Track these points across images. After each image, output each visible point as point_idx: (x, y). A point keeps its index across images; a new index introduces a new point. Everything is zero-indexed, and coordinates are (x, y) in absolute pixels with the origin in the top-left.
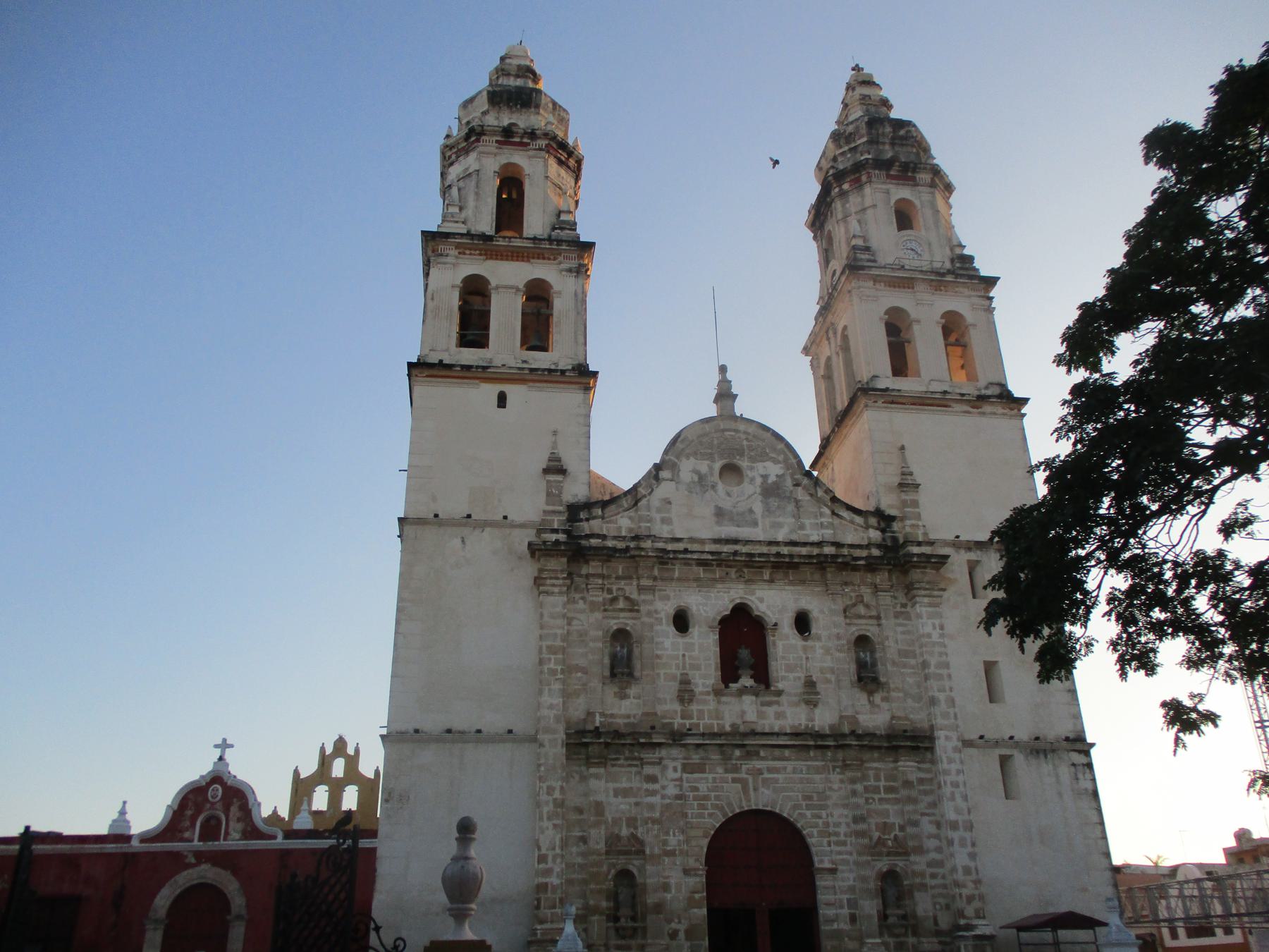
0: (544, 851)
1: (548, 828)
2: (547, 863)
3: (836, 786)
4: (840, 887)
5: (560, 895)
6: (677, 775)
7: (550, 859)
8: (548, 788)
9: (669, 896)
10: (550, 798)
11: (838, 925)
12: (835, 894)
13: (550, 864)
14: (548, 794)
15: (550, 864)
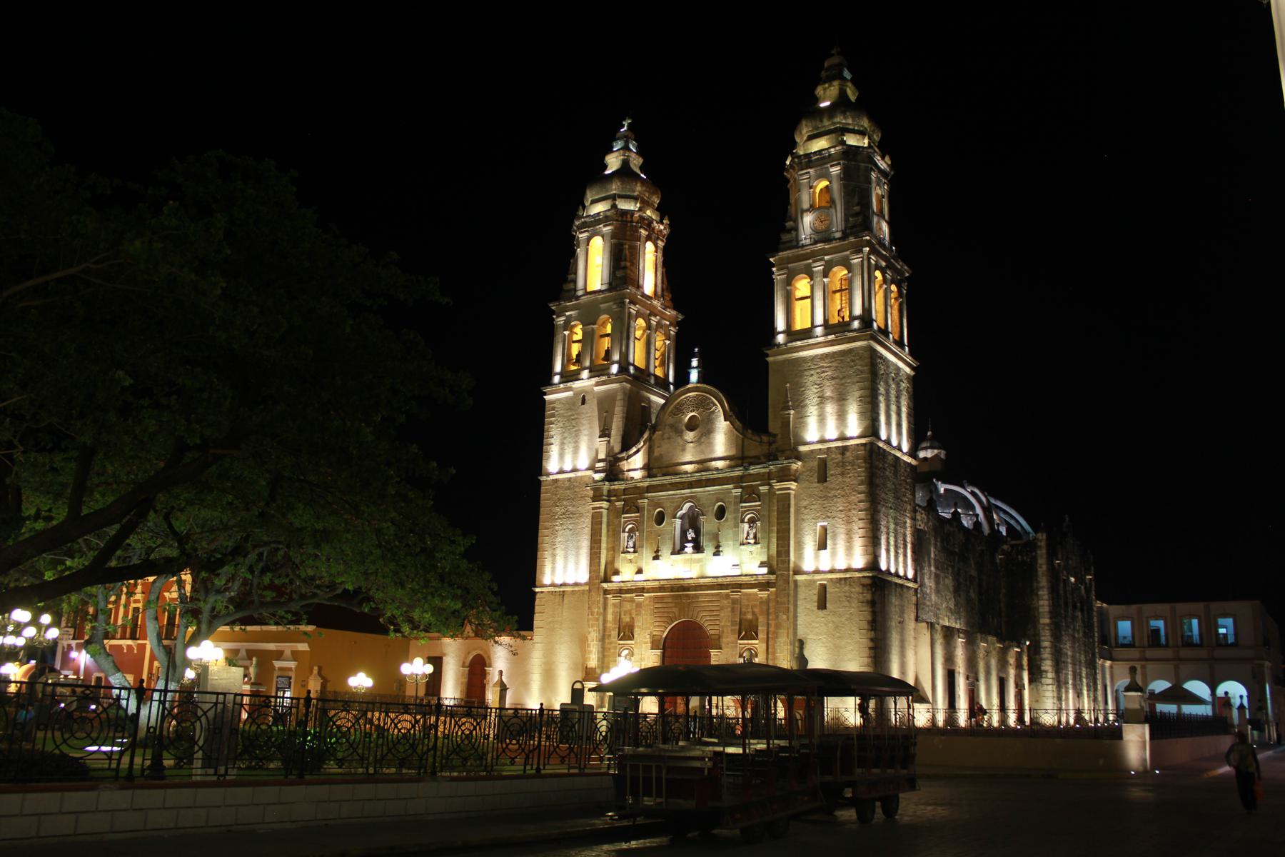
7: (592, 646)
14: (592, 615)
15: (592, 649)
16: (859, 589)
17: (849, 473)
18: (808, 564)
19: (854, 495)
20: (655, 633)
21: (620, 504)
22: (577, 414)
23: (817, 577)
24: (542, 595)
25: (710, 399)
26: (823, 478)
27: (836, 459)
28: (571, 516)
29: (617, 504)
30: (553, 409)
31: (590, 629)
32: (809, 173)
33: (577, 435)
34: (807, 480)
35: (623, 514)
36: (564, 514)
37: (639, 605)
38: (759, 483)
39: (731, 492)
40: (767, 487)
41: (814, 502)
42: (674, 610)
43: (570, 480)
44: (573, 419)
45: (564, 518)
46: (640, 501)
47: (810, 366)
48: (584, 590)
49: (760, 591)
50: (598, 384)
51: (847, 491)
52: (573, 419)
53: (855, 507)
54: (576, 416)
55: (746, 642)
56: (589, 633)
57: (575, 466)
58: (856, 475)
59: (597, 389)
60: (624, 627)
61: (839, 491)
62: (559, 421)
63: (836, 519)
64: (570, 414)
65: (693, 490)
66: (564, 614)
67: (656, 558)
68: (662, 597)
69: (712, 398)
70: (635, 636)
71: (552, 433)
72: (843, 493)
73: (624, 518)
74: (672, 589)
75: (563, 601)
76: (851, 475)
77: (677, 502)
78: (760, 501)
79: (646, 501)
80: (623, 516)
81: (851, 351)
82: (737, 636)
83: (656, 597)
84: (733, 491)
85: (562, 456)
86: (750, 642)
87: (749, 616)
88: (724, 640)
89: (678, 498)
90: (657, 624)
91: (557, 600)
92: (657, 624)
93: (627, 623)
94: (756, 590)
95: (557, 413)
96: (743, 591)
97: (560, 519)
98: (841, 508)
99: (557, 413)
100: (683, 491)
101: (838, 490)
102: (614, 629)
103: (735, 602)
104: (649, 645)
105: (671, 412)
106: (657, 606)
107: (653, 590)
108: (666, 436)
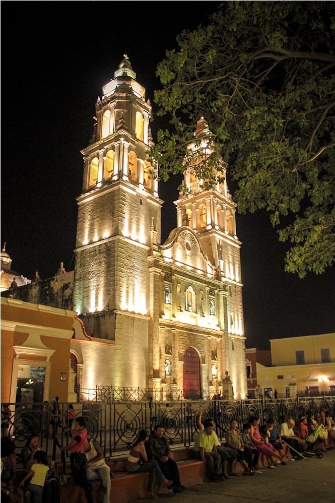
16: (241, 344)
18: (229, 332)
20: (180, 352)
23: (232, 336)
24: (120, 317)
30: (125, 196)
33: (138, 221)
36: (132, 266)
37: (174, 335)
38: (215, 288)
42: (188, 341)
43: (135, 246)
48: (146, 320)
50: (149, 197)
56: (154, 347)
57: (138, 239)
59: (148, 200)
64: (134, 205)
65: (193, 281)
66: (134, 332)
68: (183, 333)
71: (125, 211)
73: (165, 283)
74: (187, 329)
75: (133, 324)
79: (175, 277)
81: (235, 247)
83: (180, 332)
85: (130, 228)
87: (213, 349)
88: (206, 359)
90: (181, 347)
91: (130, 322)
92: (181, 347)
94: (215, 337)
103: (210, 341)
106: (181, 337)
107: (182, 328)
108: (179, 246)
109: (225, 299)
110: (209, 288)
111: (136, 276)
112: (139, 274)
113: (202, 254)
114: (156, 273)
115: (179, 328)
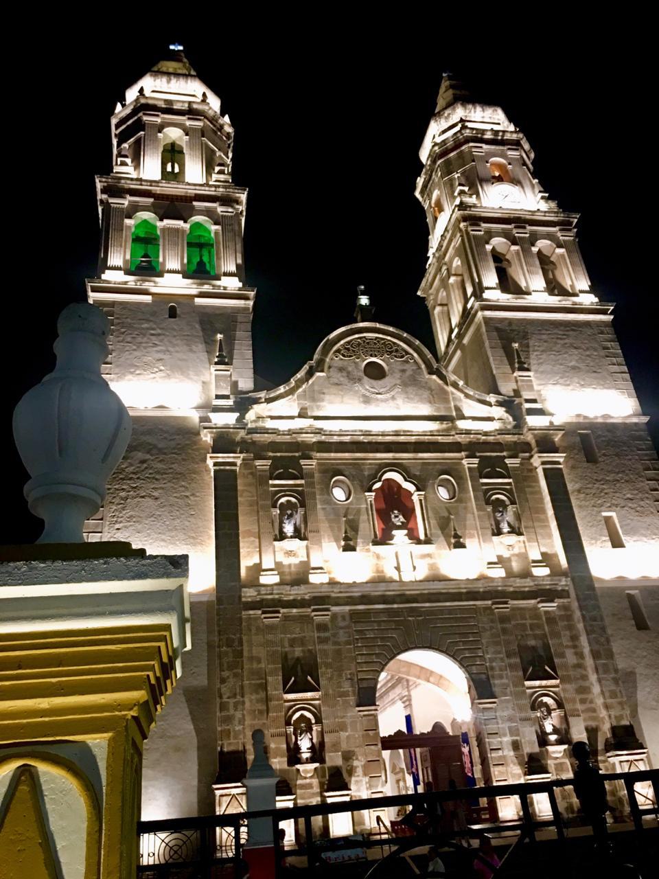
0: (225, 700)
1: (228, 677)
2: (228, 710)
3: (487, 626)
4: (500, 716)
5: (242, 741)
6: (346, 623)
7: (231, 706)
8: (227, 639)
9: (343, 735)
10: (229, 649)
11: (503, 752)
12: (498, 723)
13: (232, 712)
14: (228, 646)
15: (232, 712)
17: (627, 455)
19: (642, 482)
21: (262, 464)
22: (160, 329)
25: (398, 345)
26: (591, 458)
27: (604, 436)
28: (157, 477)
29: (258, 463)
31: (226, 674)
32: (481, 147)
34: (572, 458)
35: (271, 479)
38: (505, 454)
39: (461, 464)
40: (518, 461)
41: (588, 486)
44: (153, 335)
45: (138, 478)
46: (302, 462)
47: (539, 330)
49: (542, 601)
51: (632, 476)
52: (153, 335)
53: (647, 495)
54: (159, 331)
55: (537, 683)
58: (637, 457)
60: (294, 667)
61: (620, 475)
62: (123, 333)
63: (625, 508)
67: (349, 548)
69: (401, 344)
70: (323, 682)
72: (627, 478)
76: (630, 457)
77: (369, 469)
78: (510, 478)
79: (314, 462)
80: (271, 482)
82: (521, 673)
83: (353, 614)
84: (465, 462)
86: (544, 683)
89: (370, 464)
93: (298, 659)
94: (533, 601)
95: (118, 321)
96: (511, 602)
97: (131, 479)
98: (629, 496)
99: (118, 321)
100: (379, 455)
101: (618, 473)
102: (273, 673)
103: (504, 619)
104: (352, 699)
105: (338, 351)
109: (555, 478)
110: (476, 461)
111: (156, 494)
112: (169, 484)
113: (434, 377)
114: (222, 467)
115: (337, 602)
